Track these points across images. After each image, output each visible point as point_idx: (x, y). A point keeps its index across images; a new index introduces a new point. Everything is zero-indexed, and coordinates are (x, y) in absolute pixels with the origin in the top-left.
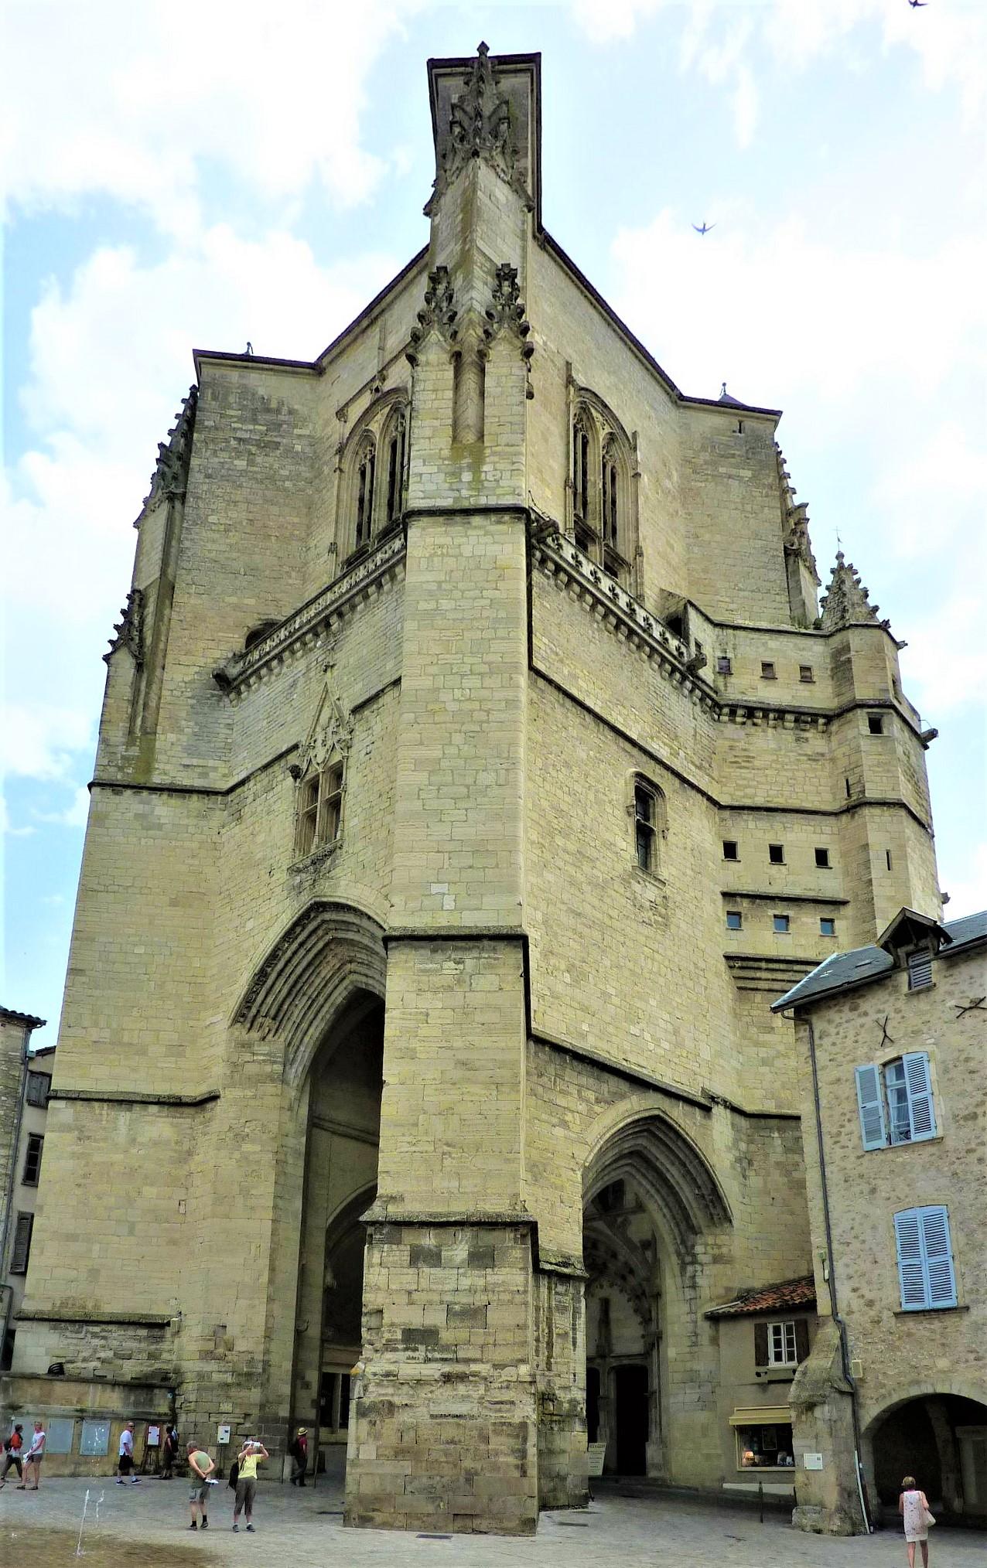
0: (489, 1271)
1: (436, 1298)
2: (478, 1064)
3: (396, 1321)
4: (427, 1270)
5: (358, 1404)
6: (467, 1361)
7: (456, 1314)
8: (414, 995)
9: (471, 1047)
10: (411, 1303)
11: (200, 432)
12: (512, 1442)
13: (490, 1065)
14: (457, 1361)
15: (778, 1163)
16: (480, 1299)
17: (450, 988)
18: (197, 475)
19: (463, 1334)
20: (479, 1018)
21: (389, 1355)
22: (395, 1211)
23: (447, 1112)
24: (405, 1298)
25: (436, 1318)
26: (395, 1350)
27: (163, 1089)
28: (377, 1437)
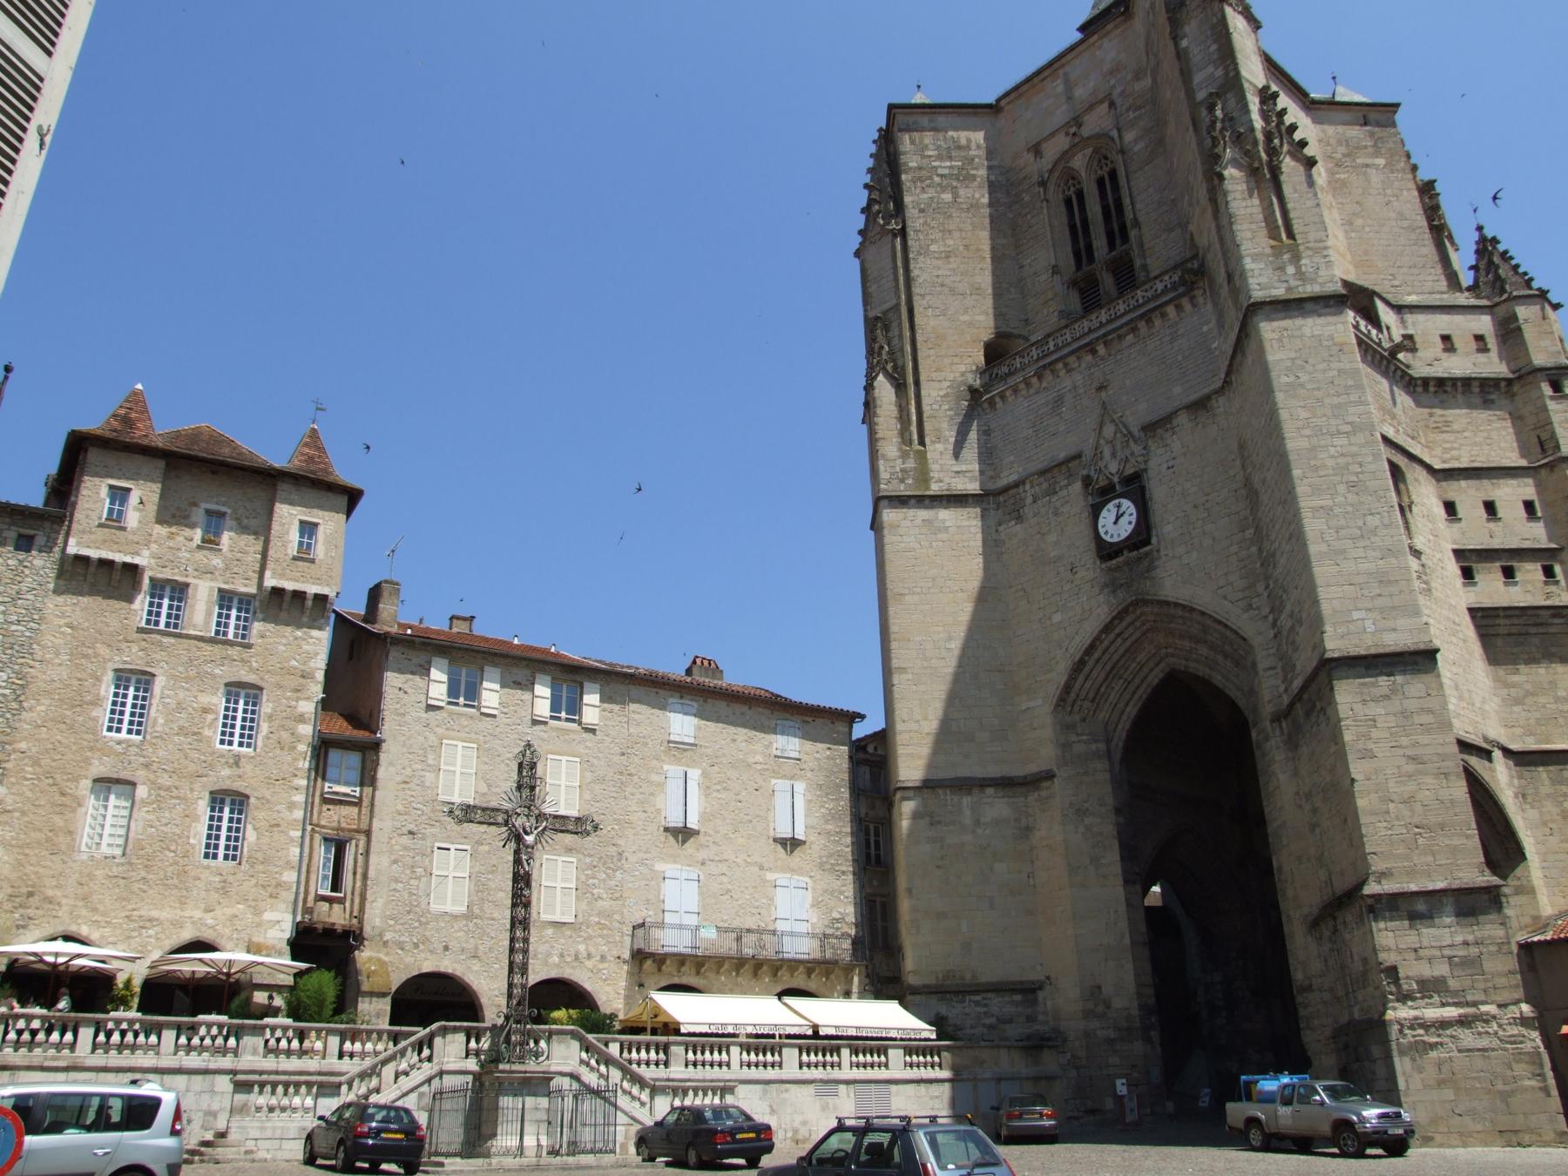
0: (1475, 928)
1: (1438, 953)
2: (1425, 758)
3: (1410, 974)
4: (1424, 931)
5: (1398, 1044)
6: (1475, 1004)
7: (1456, 965)
8: (1360, 705)
9: (1416, 744)
10: (1418, 959)
11: (906, 173)
12: (1531, 1068)
13: (1435, 759)
14: (1468, 1004)
15: (1548, 795)
16: (1474, 951)
17: (1387, 697)
18: (912, 211)
19: (1467, 982)
20: (1417, 719)
21: (1410, 1003)
22: (1389, 887)
23: (1409, 801)
24: (1412, 955)
25: (1442, 969)
26: (1414, 999)
27: (994, 771)
28: (1420, 1070)
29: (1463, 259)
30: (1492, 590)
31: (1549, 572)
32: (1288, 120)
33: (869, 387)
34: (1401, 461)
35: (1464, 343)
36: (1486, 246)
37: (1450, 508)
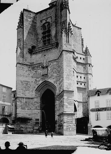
29: (84, 49)
30: (79, 85)
31: (85, 85)
32: (71, 28)
33: (17, 48)
34: (74, 71)
35: (82, 59)
36: (87, 48)
37: (77, 76)
